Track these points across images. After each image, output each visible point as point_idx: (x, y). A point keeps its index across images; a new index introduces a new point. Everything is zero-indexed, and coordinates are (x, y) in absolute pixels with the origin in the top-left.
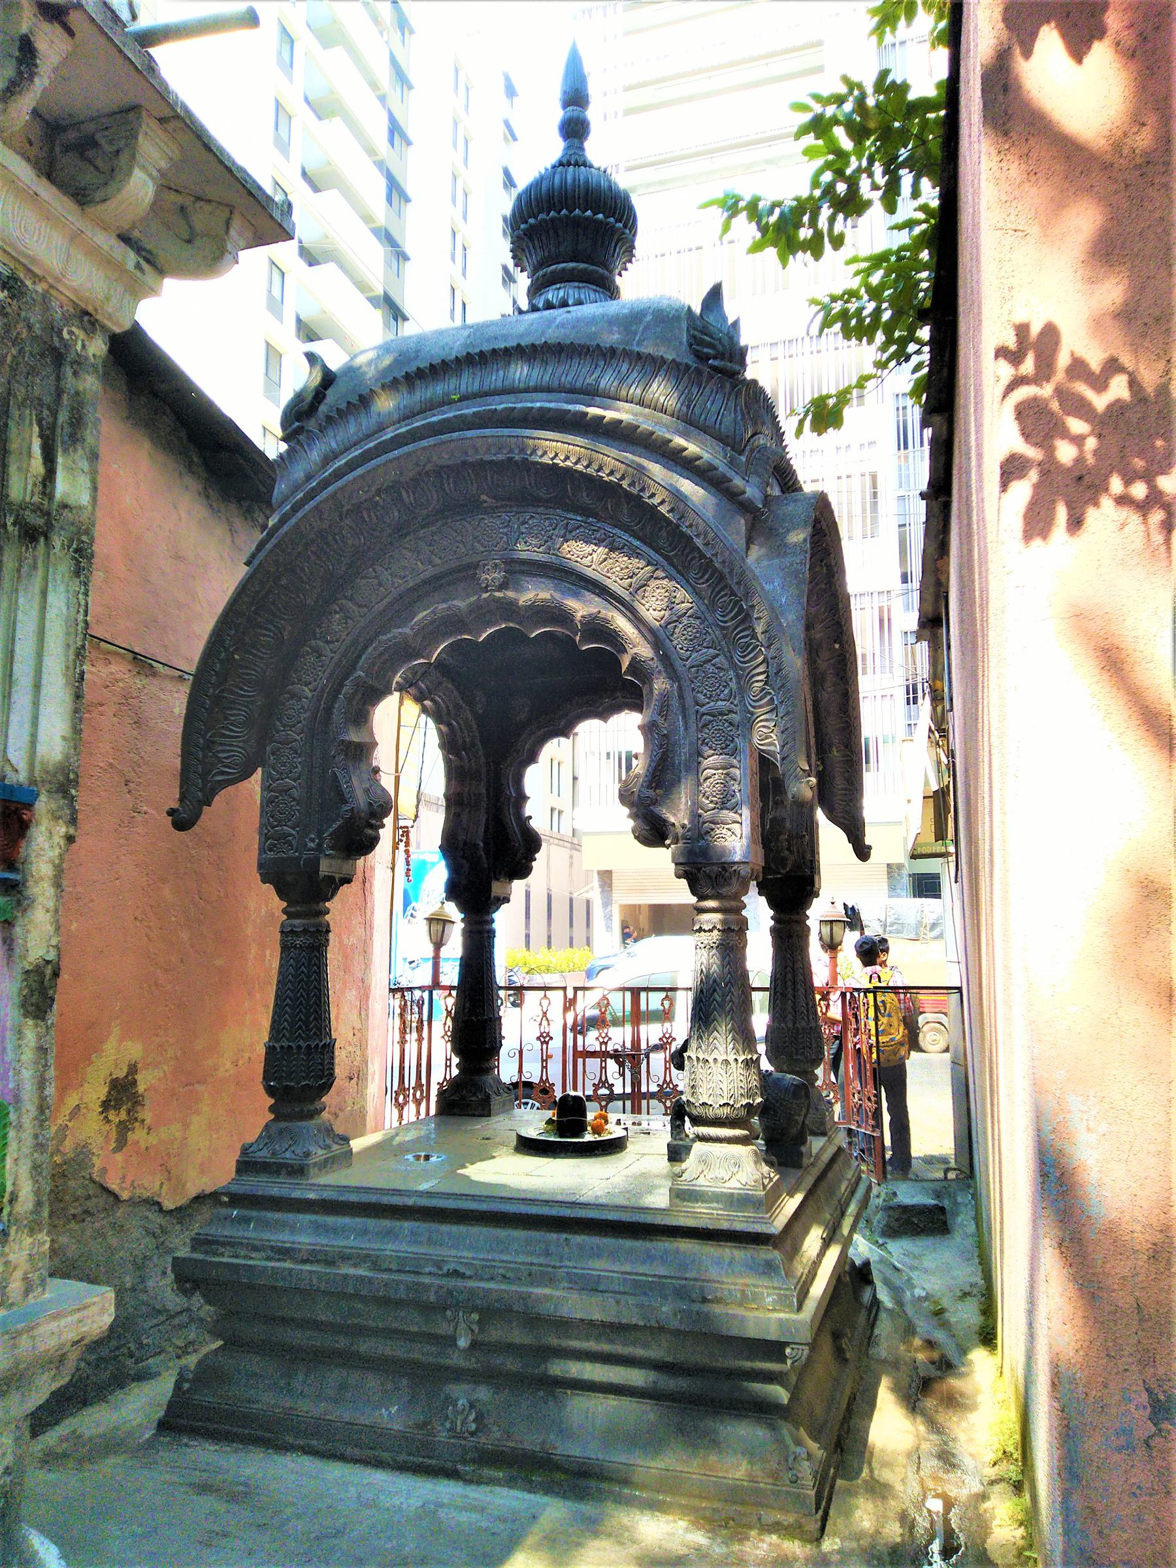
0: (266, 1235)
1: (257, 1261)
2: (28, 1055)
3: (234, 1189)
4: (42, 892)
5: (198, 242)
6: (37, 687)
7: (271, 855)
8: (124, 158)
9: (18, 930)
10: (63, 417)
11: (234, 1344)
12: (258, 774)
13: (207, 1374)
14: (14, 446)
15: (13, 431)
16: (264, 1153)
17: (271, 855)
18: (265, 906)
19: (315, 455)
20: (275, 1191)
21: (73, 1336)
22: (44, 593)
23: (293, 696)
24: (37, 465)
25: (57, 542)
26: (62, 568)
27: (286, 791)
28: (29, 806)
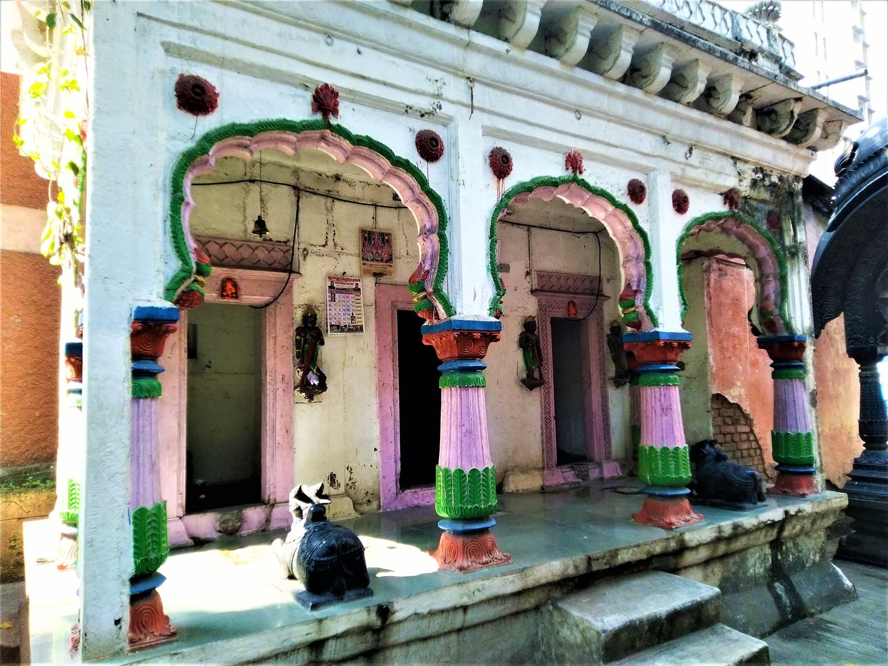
0: (874, 492)
1: (871, 500)
2: (814, 419)
3: (854, 474)
4: (810, 368)
5: (830, 137)
6: (801, 304)
7: (852, 346)
8: (811, 126)
9: (806, 380)
10: (796, 214)
11: (860, 531)
12: (842, 314)
13: (850, 541)
14: (785, 228)
15: (784, 224)
16: (865, 461)
17: (852, 346)
18: (855, 368)
19: (854, 180)
20: (874, 476)
21: (839, 505)
22: (799, 273)
23: (855, 281)
24: (792, 233)
25: (800, 255)
26: (802, 263)
27: (856, 320)
28: (805, 341)
